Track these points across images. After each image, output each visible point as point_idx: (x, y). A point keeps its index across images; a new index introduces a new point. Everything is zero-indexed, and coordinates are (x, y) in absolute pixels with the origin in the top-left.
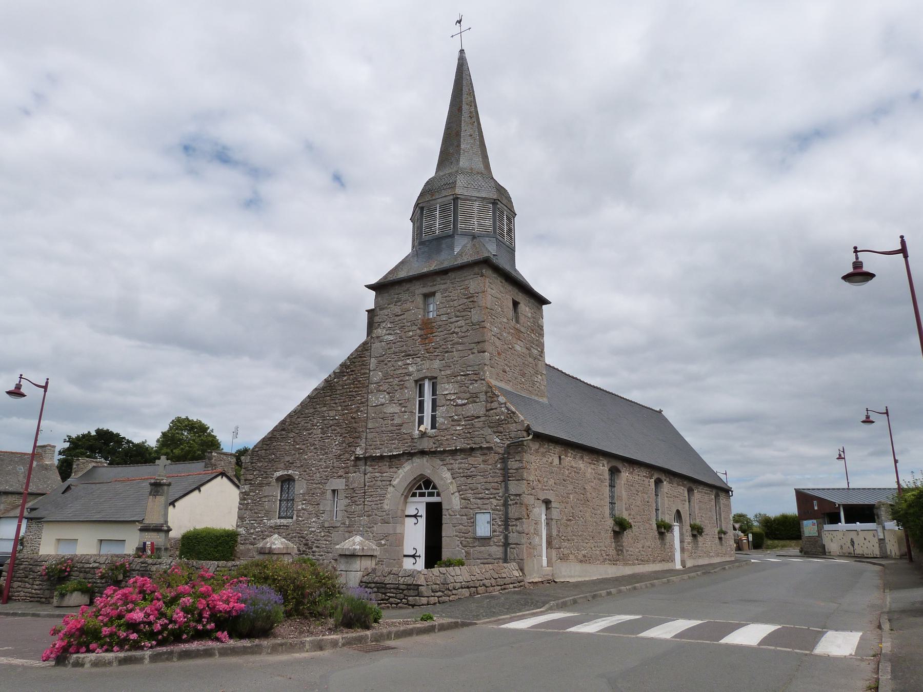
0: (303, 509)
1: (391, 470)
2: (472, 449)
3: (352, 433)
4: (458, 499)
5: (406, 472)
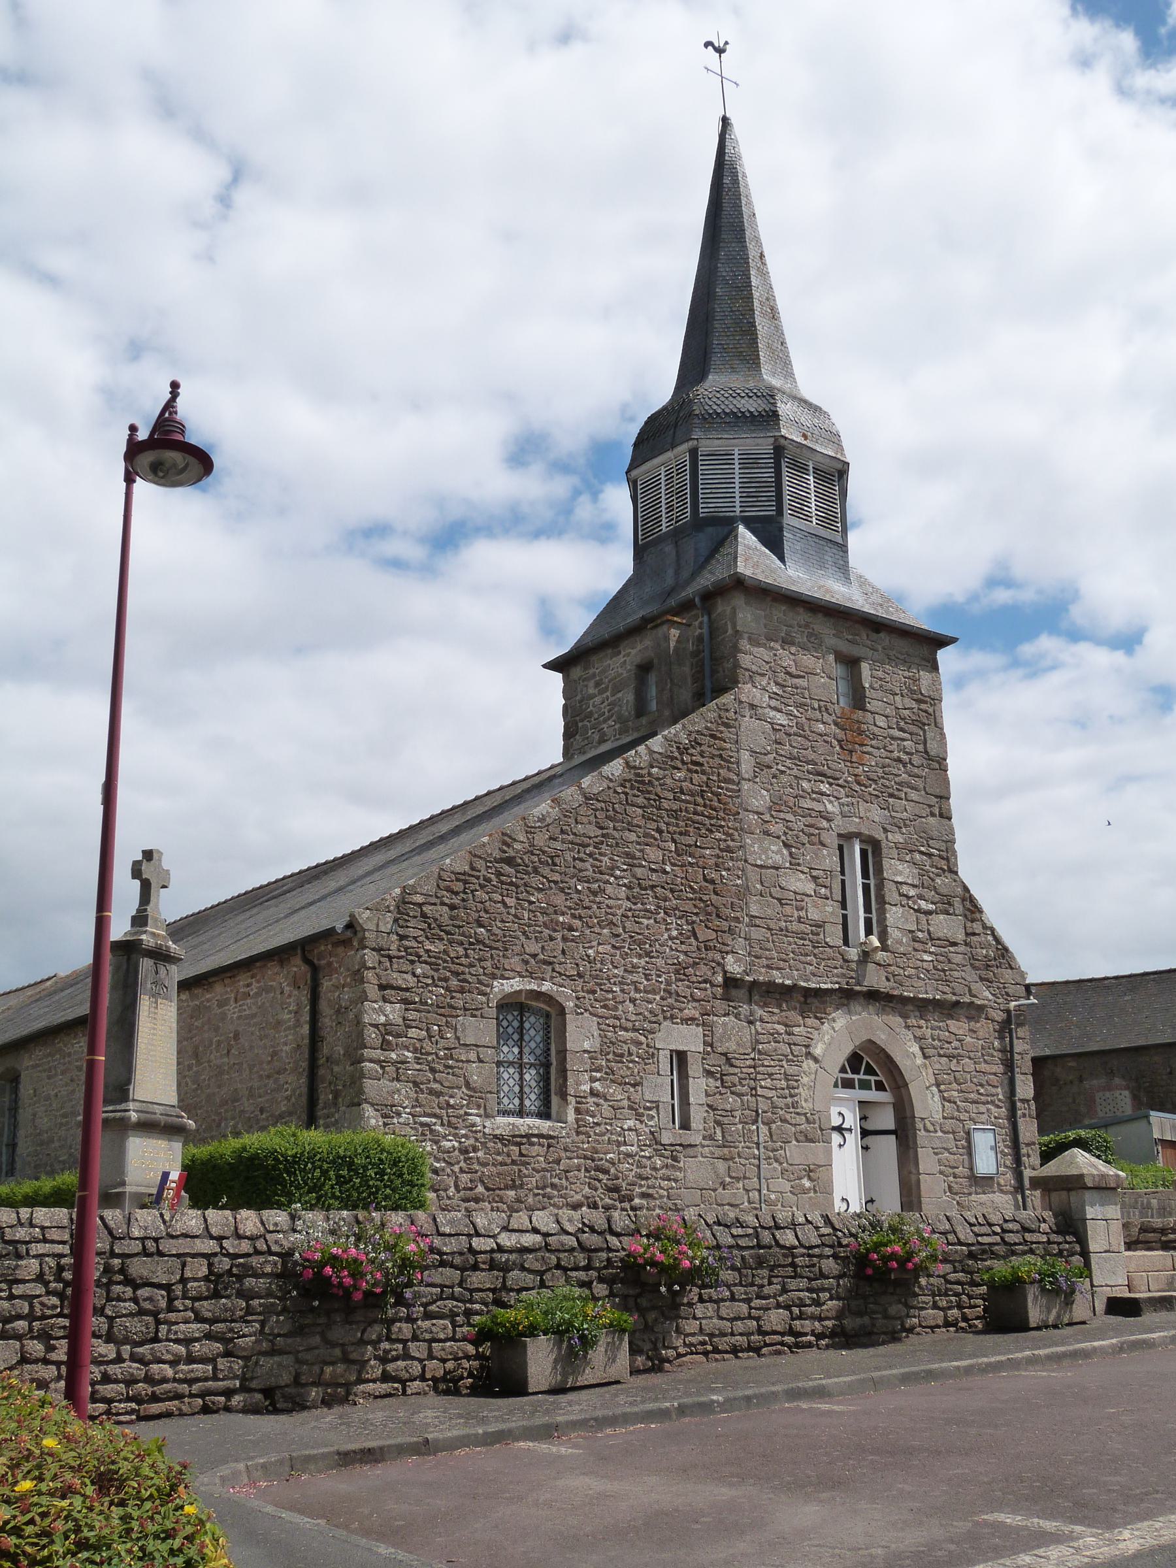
0: (593, 1093)
1: (809, 1021)
2: (957, 1004)
3: (710, 911)
4: (937, 1098)
5: (835, 1035)
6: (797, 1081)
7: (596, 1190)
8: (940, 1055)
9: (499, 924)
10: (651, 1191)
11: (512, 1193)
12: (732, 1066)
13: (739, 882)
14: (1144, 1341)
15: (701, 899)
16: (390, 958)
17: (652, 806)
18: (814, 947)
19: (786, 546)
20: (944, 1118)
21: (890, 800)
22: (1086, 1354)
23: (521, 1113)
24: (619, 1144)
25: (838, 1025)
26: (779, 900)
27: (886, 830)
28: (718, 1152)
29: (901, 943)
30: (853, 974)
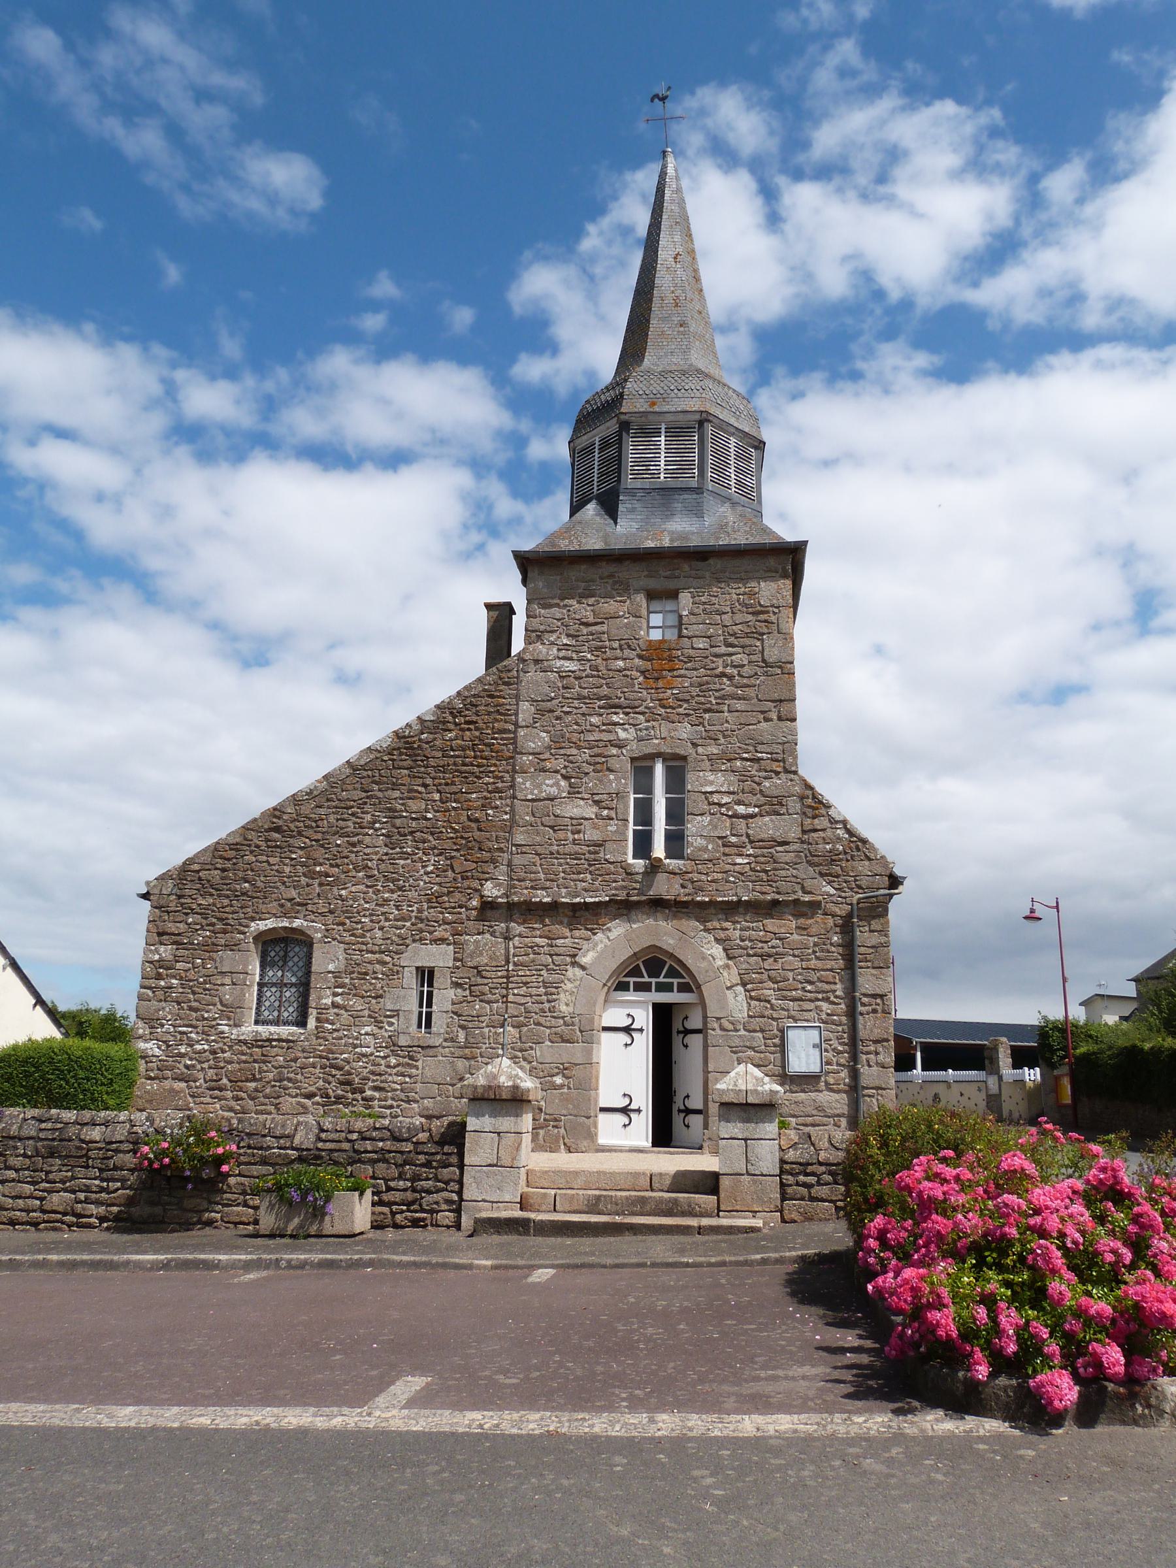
0: (335, 1005)
1: (577, 933)
2: (775, 903)
3: (473, 848)
4: (742, 997)
5: (611, 944)
6: (556, 988)
7: (329, 1083)
8: (749, 955)
9: (262, 879)
10: (382, 1085)
11: (253, 1085)
12: (483, 977)
13: (505, 817)
14: (204, 1262)
15: (462, 837)
16: (168, 912)
17: (420, 766)
18: (590, 865)
19: (621, 508)
20: (749, 1016)
21: (707, 716)
22: (215, 1266)
23: (276, 1022)
24: (355, 1046)
25: (613, 935)
26: (552, 827)
27: (695, 745)
28: (459, 1052)
29: (705, 849)
30: (638, 886)
